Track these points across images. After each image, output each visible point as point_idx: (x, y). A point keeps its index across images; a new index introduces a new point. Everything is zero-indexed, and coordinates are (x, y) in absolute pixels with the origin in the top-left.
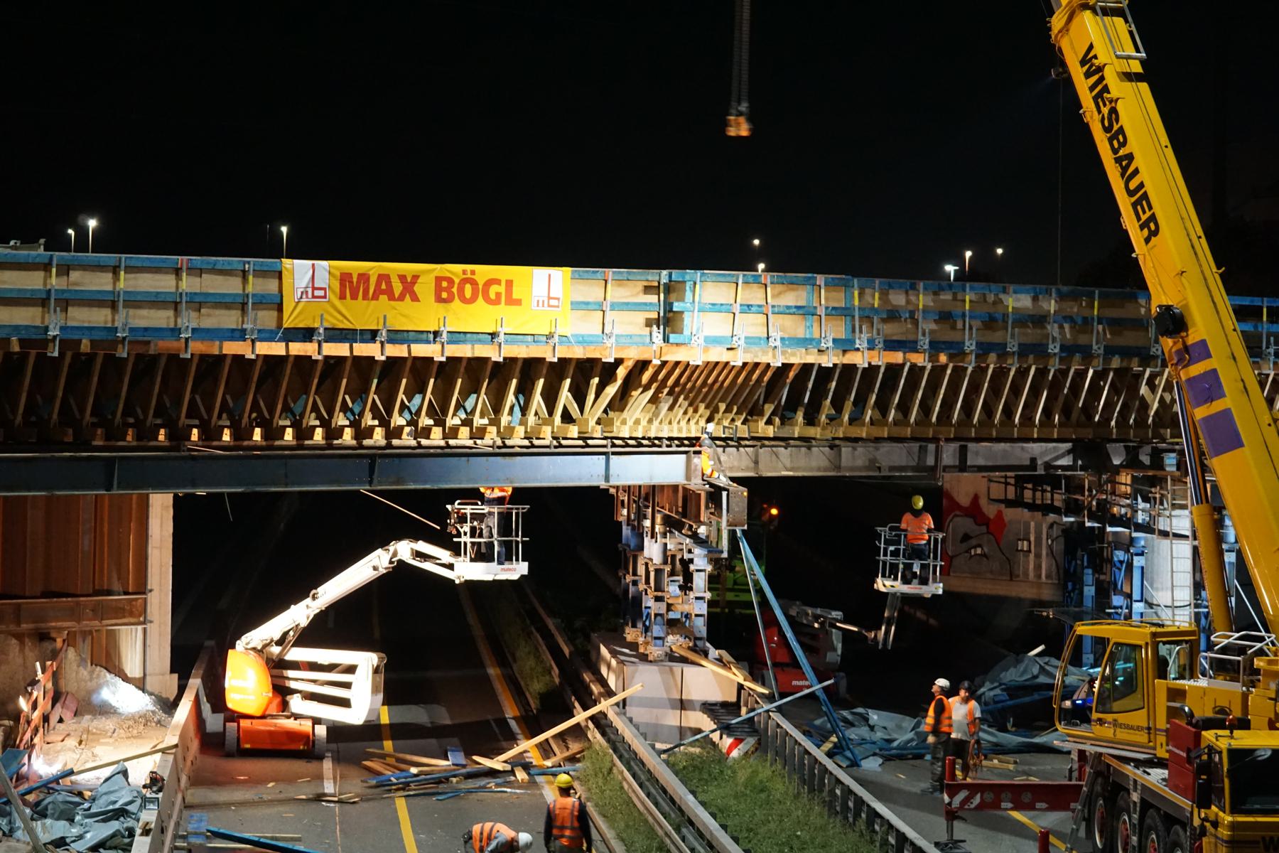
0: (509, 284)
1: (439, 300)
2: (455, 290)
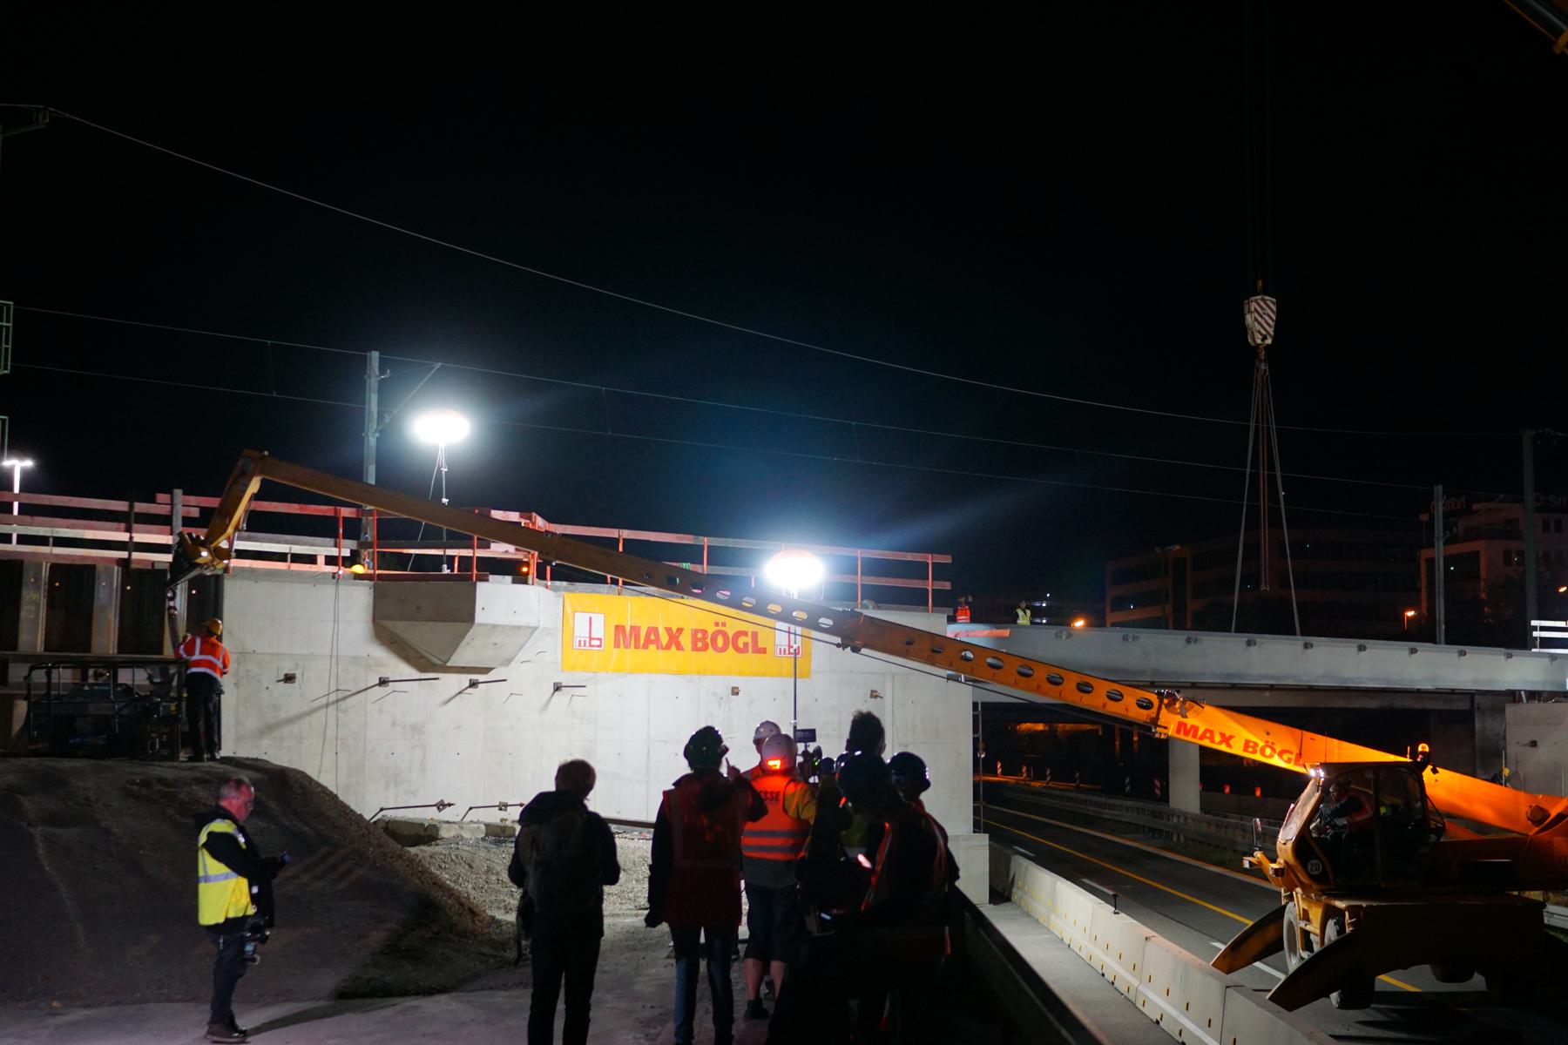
0: (755, 635)
1: (695, 648)
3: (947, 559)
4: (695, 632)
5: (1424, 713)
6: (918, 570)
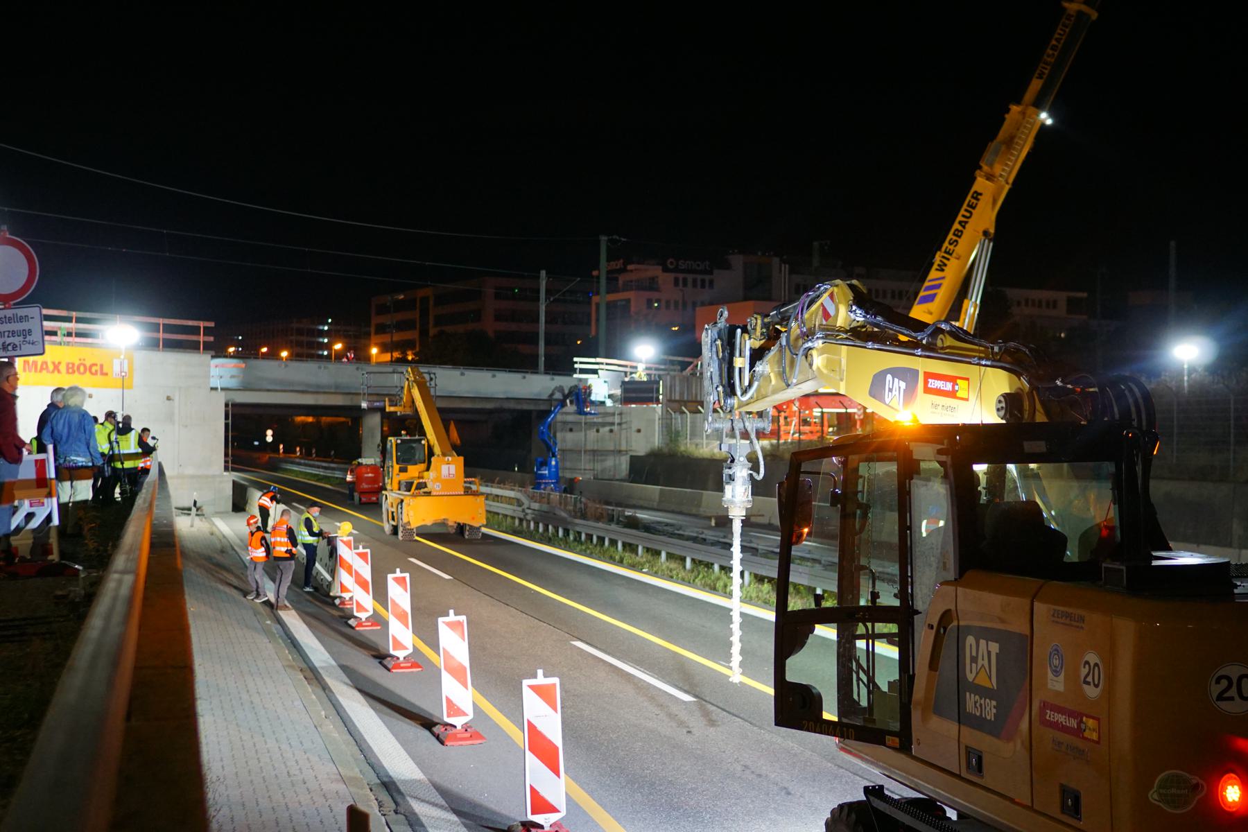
1: (68, 372)
3: (212, 324)
4: (68, 364)
5: (530, 412)
6: (195, 330)
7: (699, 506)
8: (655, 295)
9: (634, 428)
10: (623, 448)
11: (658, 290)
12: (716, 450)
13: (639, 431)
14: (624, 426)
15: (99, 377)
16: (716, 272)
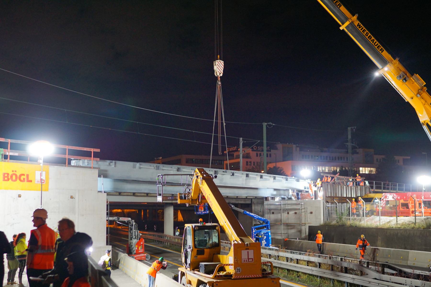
1: (4, 180)
2: (9, 177)
3: (98, 150)
7: (407, 259)
8: (249, 160)
9: (309, 211)
10: (303, 222)
11: (250, 158)
12: (378, 224)
13: (311, 213)
14: (303, 210)
15: (26, 183)
16: (272, 150)
